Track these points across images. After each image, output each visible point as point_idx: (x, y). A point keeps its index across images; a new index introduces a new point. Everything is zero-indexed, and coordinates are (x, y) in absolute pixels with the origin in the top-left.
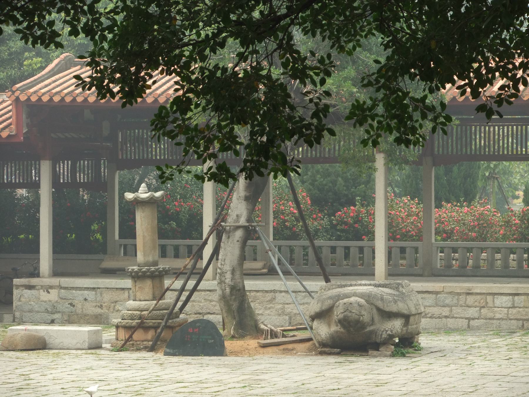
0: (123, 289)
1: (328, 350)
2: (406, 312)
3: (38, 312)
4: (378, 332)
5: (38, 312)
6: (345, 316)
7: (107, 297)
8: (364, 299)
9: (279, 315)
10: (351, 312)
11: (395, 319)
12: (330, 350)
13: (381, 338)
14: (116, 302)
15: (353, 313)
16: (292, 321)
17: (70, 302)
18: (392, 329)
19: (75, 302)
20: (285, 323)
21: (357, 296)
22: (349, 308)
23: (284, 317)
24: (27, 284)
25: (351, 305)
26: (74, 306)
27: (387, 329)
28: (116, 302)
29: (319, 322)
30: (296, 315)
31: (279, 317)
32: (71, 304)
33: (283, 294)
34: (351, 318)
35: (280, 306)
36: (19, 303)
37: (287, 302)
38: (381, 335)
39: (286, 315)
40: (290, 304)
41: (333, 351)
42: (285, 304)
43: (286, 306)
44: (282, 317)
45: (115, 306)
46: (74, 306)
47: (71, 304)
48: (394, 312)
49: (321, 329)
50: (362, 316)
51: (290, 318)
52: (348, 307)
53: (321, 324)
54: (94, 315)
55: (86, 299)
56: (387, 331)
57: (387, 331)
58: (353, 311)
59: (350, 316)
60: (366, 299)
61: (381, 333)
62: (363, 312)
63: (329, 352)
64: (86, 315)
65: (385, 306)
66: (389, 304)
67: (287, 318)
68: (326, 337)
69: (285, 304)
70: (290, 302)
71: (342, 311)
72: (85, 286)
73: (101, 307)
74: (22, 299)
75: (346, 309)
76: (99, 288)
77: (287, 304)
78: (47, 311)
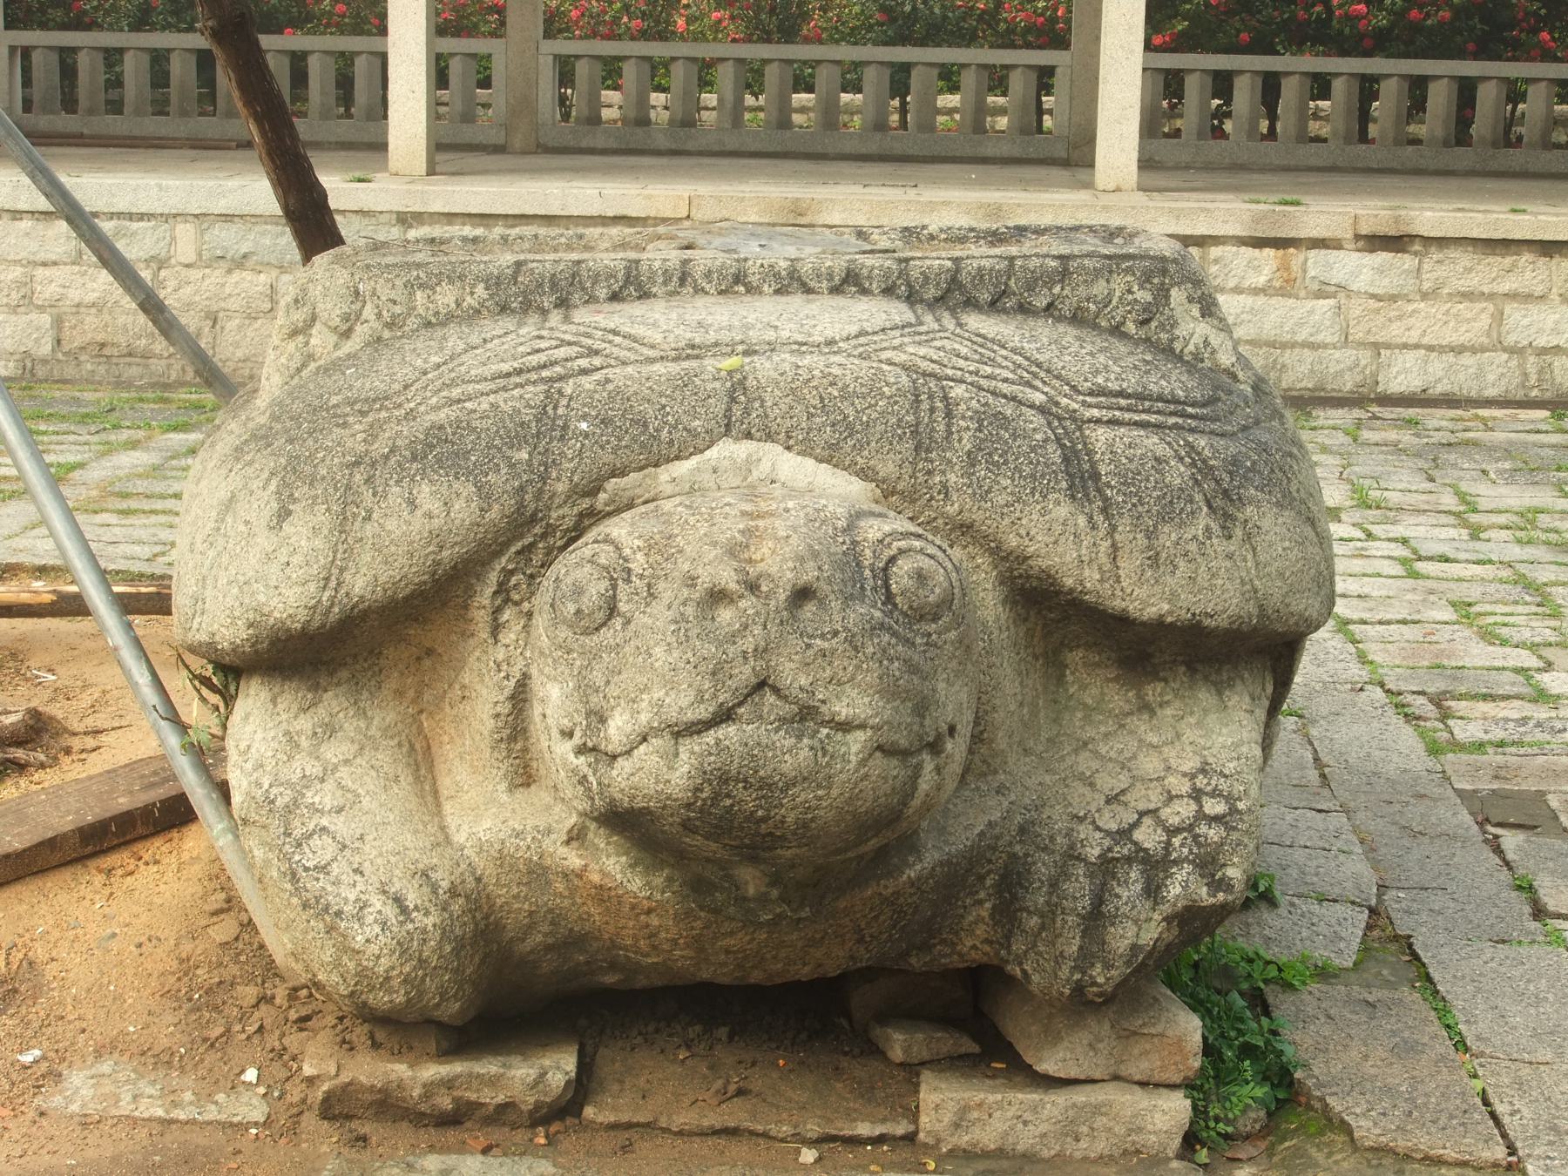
1: (430, 1089)
4: (1043, 867)
6: (719, 780)
8: (865, 474)
9: (14, 309)
10: (806, 715)
11: (1205, 696)
12: (449, 1084)
13: (1085, 959)
15: (845, 727)
16: (66, 333)
18: (1213, 833)
20: (37, 340)
21: (770, 437)
22: (791, 674)
23: (34, 316)
25: (809, 609)
27: (1149, 837)
29: (305, 723)
30: (83, 310)
31: (13, 318)
33: (26, 224)
34: (805, 795)
35: (17, 272)
37: (41, 257)
38: (1096, 919)
39: (41, 309)
40: (55, 263)
41: (492, 1098)
42: (35, 264)
43: (40, 272)
44: (24, 318)
48: (1222, 622)
49: (338, 824)
51: (58, 322)
52: (761, 652)
53: (333, 752)
56: (1156, 867)
57: (1156, 867)
58: (842, 710)
59: (804, 778)
60: (887, 468)
61: (1079, 889)
63: (445, 1102)
65: (1128, 565)
66: (1168, 536)
67: (45, 320)
68: (403, 948)
69: (35, 264)
70: (54, 257)
71: (683, 703)
75: (744, 674)
77: (44, 264)
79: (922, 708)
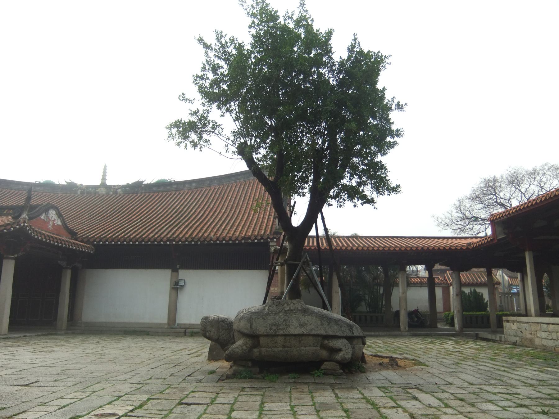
0: (538, 323)
2: (246, 331)
3: (512, 336)
5: (512, 336)
7: (534, 328)
14: (536, 331)
17: (521, 330)
19: (523, 330)
24: (506, 319)
26: (522, 333)
28: (536, 331)
32: (521, 332)
36: (506, 330)
45: (537, 334)
46: (522, 333)
47: (521, 332)
50: (207, 331)
54: (530, 339)
55: (526, 329)
62: (209, 328)
64: (527, 339)
72: (525, 321)
73: (531, 334)
74: (507, 328)
76: (529, 322)
78: (514, 336)
79: (205, 328)
